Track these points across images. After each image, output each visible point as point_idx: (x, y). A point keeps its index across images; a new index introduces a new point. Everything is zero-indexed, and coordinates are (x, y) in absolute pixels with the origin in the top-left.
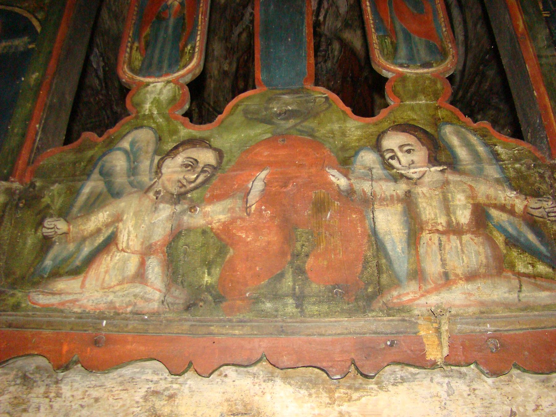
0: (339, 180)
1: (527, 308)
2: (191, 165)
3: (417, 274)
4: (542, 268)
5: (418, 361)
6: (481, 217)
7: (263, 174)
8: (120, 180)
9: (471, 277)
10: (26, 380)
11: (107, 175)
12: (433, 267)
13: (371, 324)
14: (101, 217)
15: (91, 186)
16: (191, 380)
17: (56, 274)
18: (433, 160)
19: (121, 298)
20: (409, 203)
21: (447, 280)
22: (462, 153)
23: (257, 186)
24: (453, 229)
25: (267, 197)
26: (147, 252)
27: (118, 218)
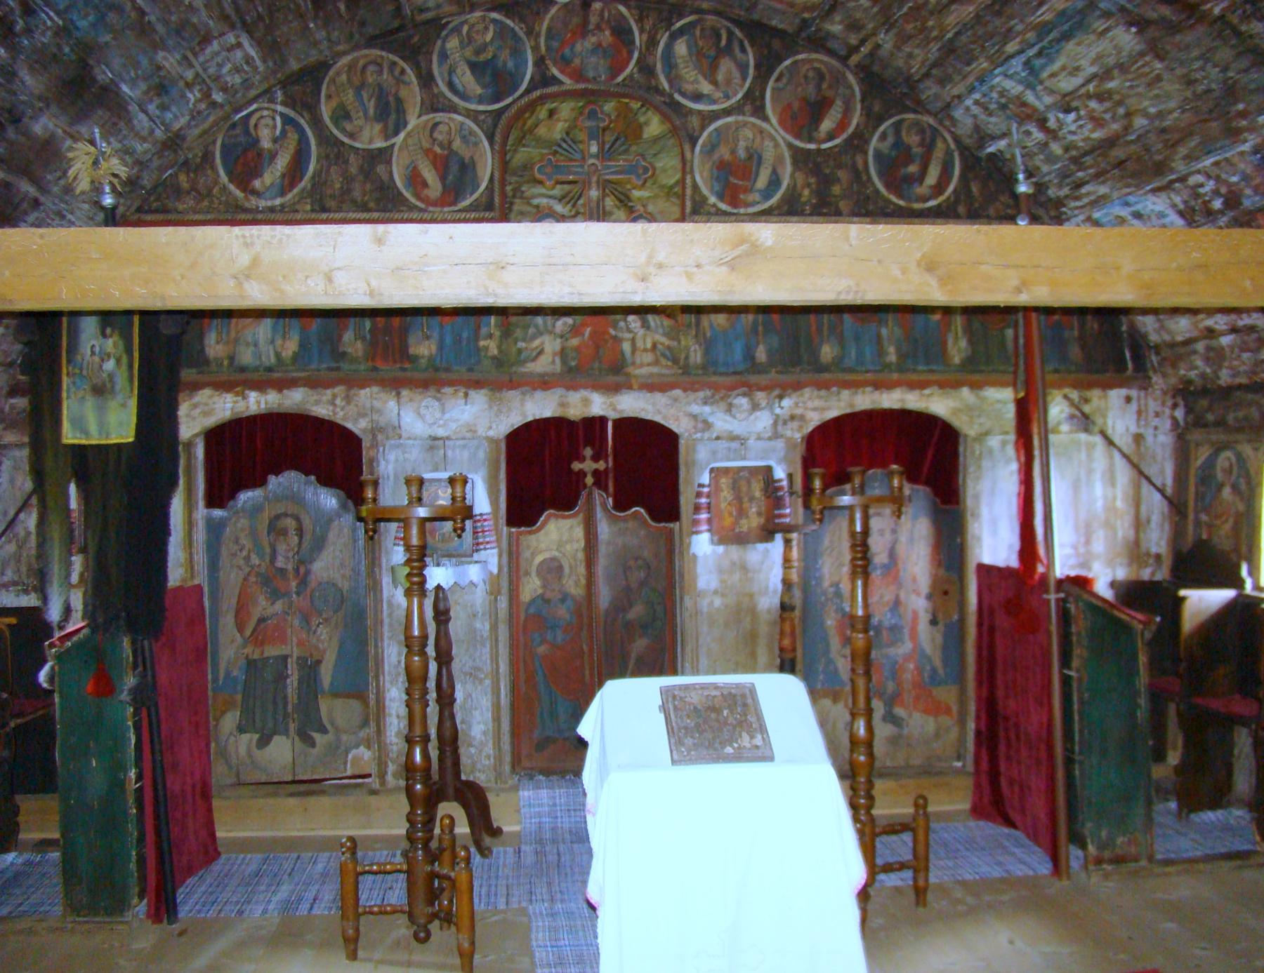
0: (612, 332)
1: (663, 375)
2: (565, 324)
3: (633, 363)
4: (669, 363)
5: (630, 388)
6: (654, 346)
7: (589, 329)
8: (542, 328)
9: (649, 365)
10: (524, 394)
11: (536, 326)
12: (638, 362)
13: (620, 379)
14: (536, 343)
15: (531, 331)
16: (571, 393)
17: (525, 362)
18: (643, 326)
19: (549, 369)
20: (633, 340)
21: (641, 366)
22: (652, 324)
23: (587, 334)
24: (645, 350)
25: (592, 335)
26: (555, 354)
27: (543, 343)
